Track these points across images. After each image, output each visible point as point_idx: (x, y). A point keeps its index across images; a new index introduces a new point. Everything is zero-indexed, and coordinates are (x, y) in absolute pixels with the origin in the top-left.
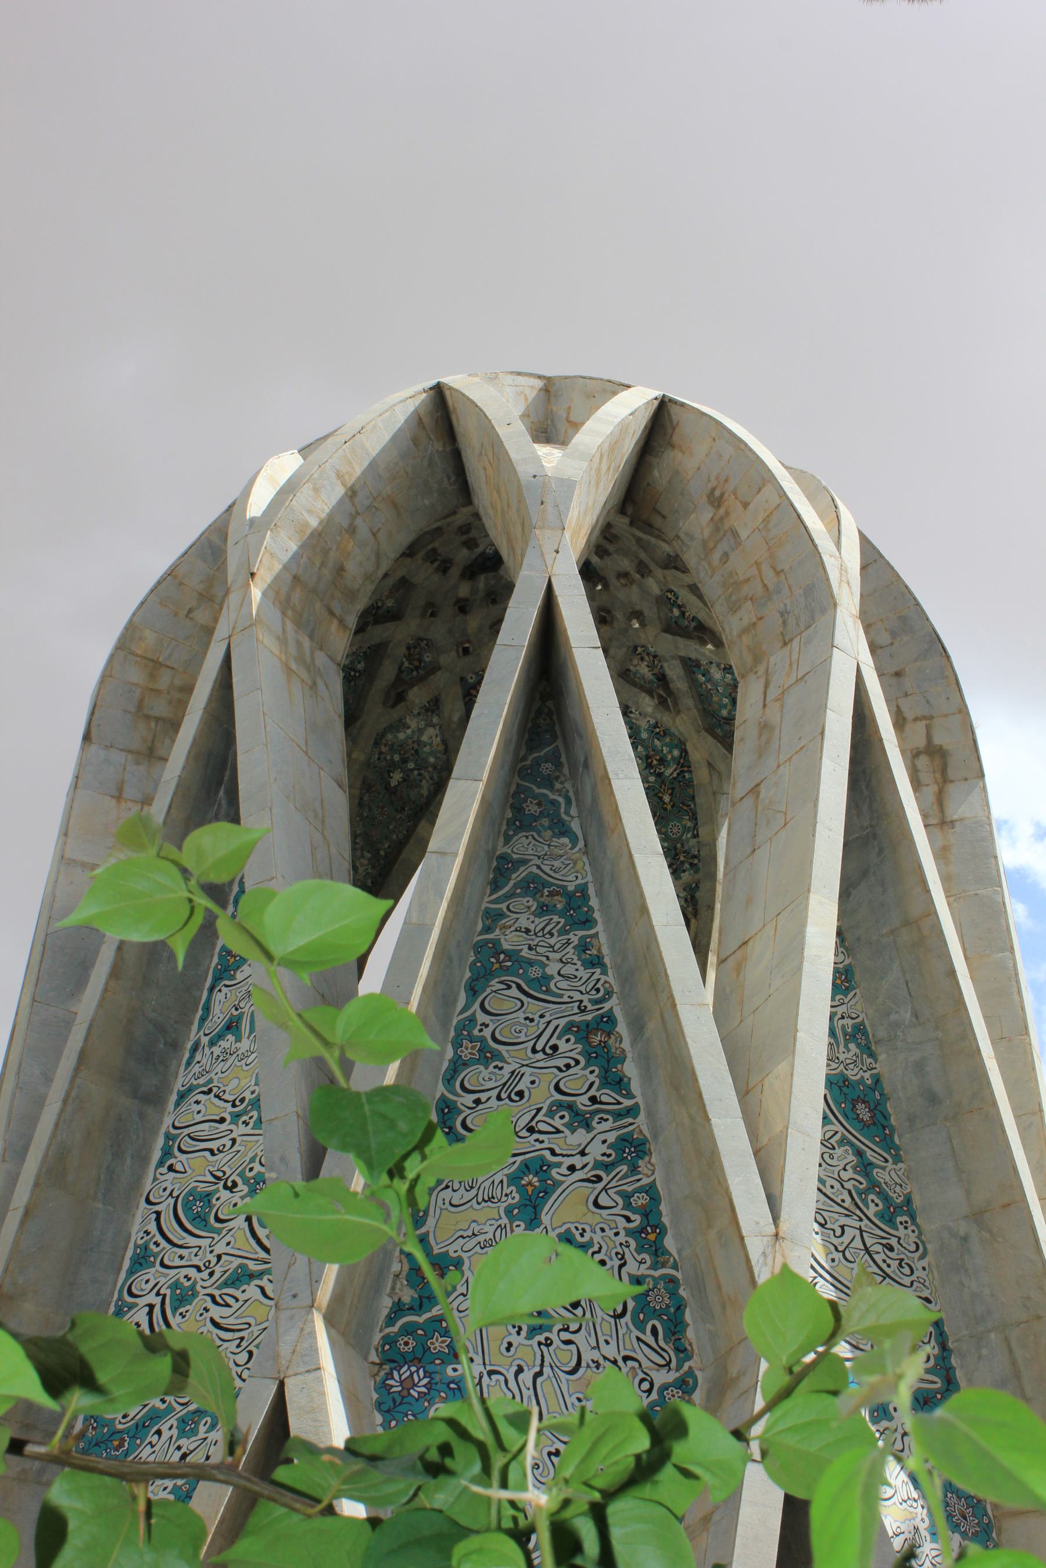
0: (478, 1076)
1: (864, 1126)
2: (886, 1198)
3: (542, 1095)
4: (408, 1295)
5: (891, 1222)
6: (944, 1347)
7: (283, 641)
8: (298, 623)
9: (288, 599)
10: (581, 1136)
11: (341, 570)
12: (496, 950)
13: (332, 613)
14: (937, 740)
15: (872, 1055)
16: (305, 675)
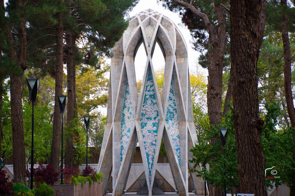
0: (126, 101)
1: (152, 98)
2: (154, 103)
3: (129, 102)
4: (123, 117)
5: (154, 105)
6: (158, 113)
7: (115, 62)
8: (117, 58)
9: (115, 57)
10: (131, 105)
11: (120, 51)
12: (126, 91)
13: (120, 55)
14: (170, 51)
15: (154, 91)
16: (118, 64)
